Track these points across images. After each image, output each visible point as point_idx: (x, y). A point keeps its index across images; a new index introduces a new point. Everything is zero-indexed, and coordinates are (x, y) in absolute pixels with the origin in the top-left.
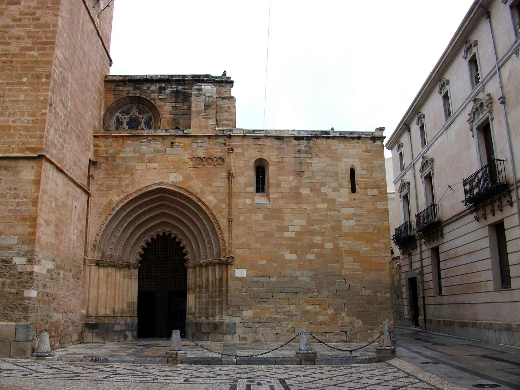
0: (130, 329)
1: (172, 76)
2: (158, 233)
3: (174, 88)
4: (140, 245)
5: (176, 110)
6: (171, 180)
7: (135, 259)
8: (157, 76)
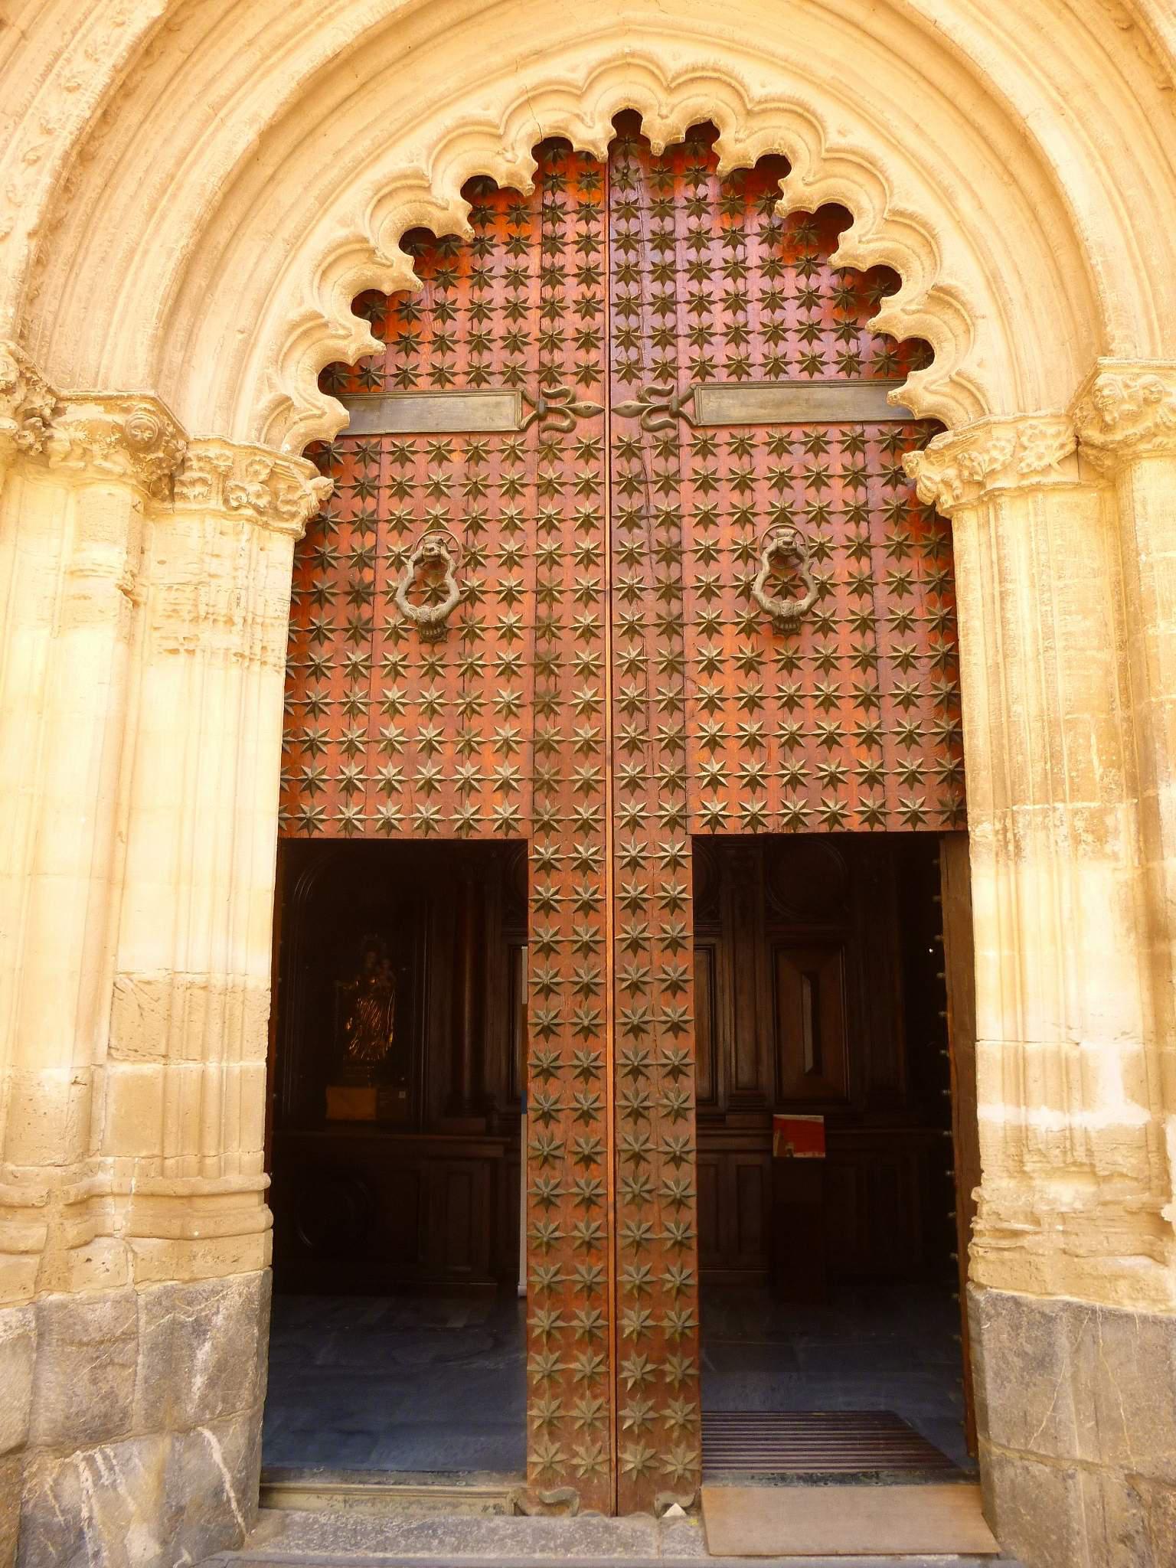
0: (135, 1400)
2: (544, 120)
4: (327, 233)
7: (252, 404)
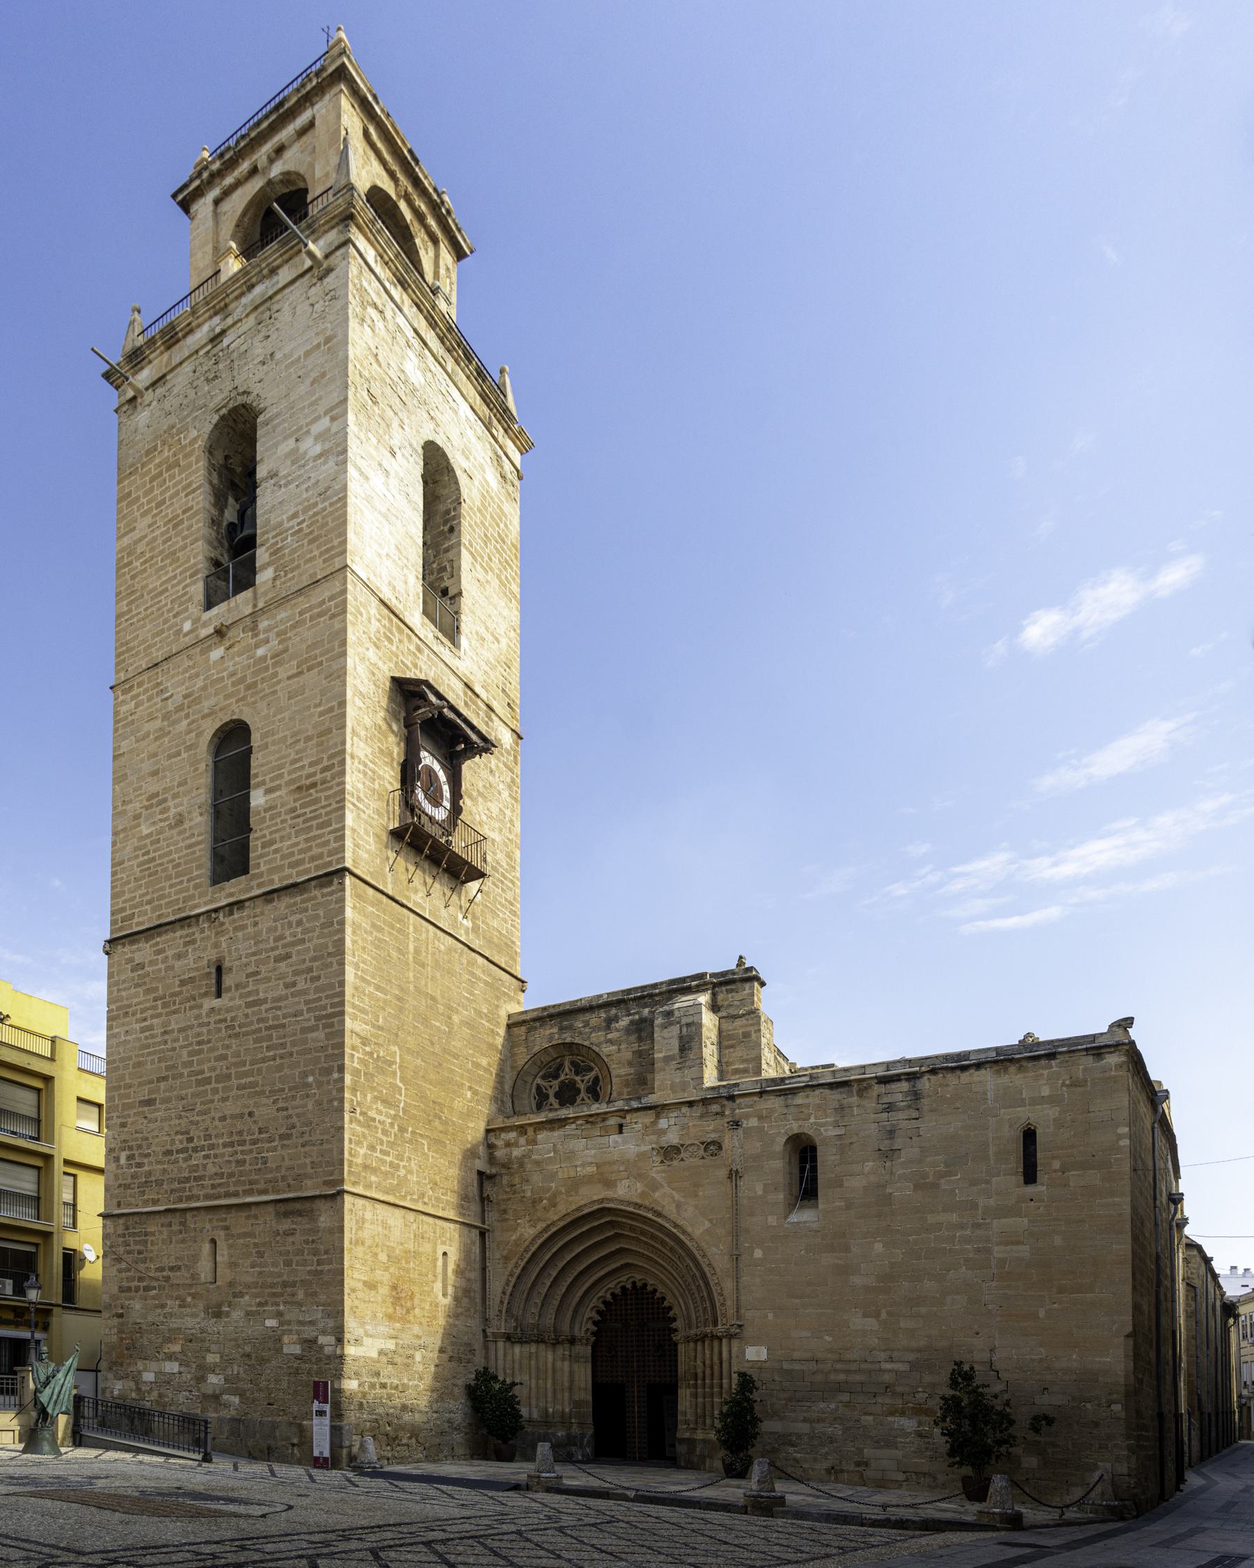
1: (629, 991)
3: (634, 1014)
5: (640, 1057)
6: (620, 1193)
8: (601, 996)
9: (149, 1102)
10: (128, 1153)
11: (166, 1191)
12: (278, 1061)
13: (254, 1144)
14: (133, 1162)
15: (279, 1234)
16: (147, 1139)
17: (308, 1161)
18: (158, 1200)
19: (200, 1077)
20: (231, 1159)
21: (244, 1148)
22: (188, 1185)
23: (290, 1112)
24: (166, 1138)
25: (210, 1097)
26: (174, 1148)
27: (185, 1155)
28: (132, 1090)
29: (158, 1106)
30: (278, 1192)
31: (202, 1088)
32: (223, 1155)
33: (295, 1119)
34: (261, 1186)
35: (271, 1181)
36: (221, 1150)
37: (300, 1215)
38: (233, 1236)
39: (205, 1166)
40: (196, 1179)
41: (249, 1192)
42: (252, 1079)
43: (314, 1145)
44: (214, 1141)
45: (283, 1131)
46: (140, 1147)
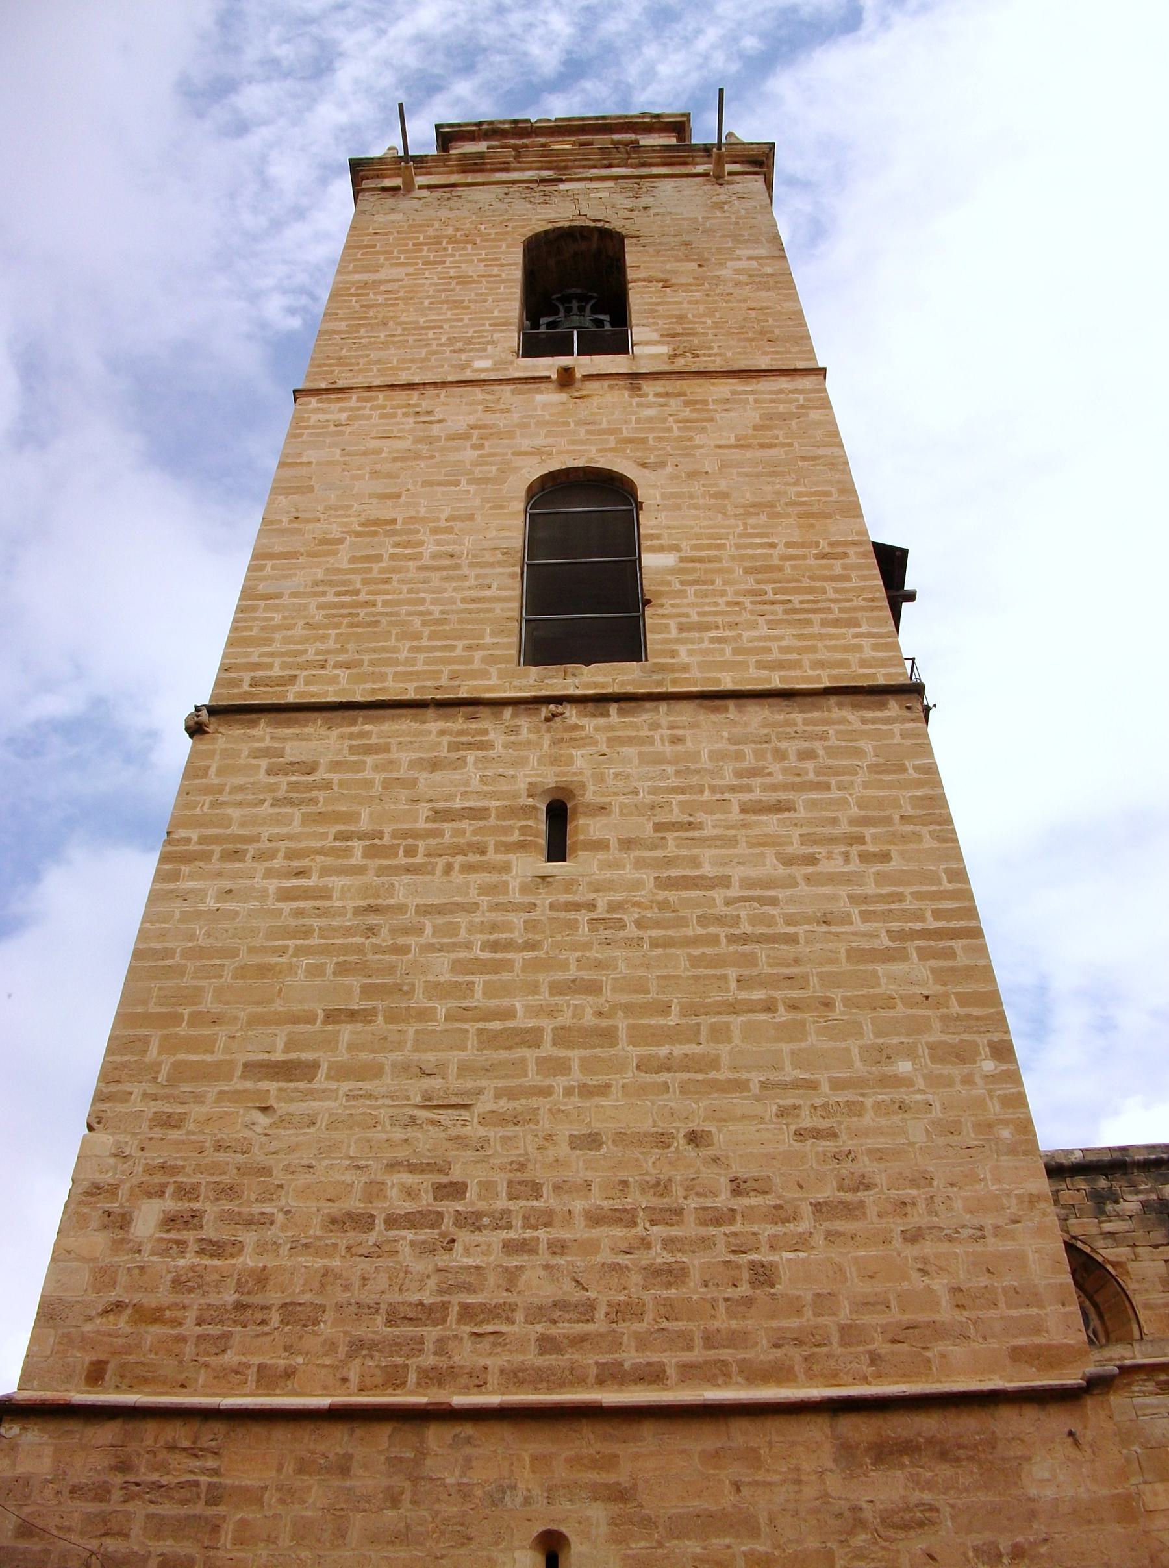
9: (286, 1070)
10: (171, 1204)
11: (332, 1346)
12: (783, 1015)
13: (718, 1221)
14: (190, 1236)
15: (860, 1524)
16: (265, 1171)
17: (939, 1284)
18: (289, 1374)
19: (496, 1025)
20: (623, 1260)
21: (675, 1232)
22: (432, 1333)
23: (846, 1142)
24: (348, 1177)
25: (533, 1078)
26: (379, 1208)
27: (425, 1235)
28: (222, 1032)
29: (321, 1081)
30: (833, 1378)
31: (504, 1054)
32: (591, 1247)
33: (865, 1165)
34: (762, 1353)
35: (798, 1342)
36: (579, 1231)
37: (944, 1456)
38: (648, 1523)
39: (511, 1277)
40: (467, 1313)
41: (718, 1373)
42: (691, 1049)
43: (950, 1239)
44: (549, 1200)
45: (827, 1192)
46: (229, 1191)
